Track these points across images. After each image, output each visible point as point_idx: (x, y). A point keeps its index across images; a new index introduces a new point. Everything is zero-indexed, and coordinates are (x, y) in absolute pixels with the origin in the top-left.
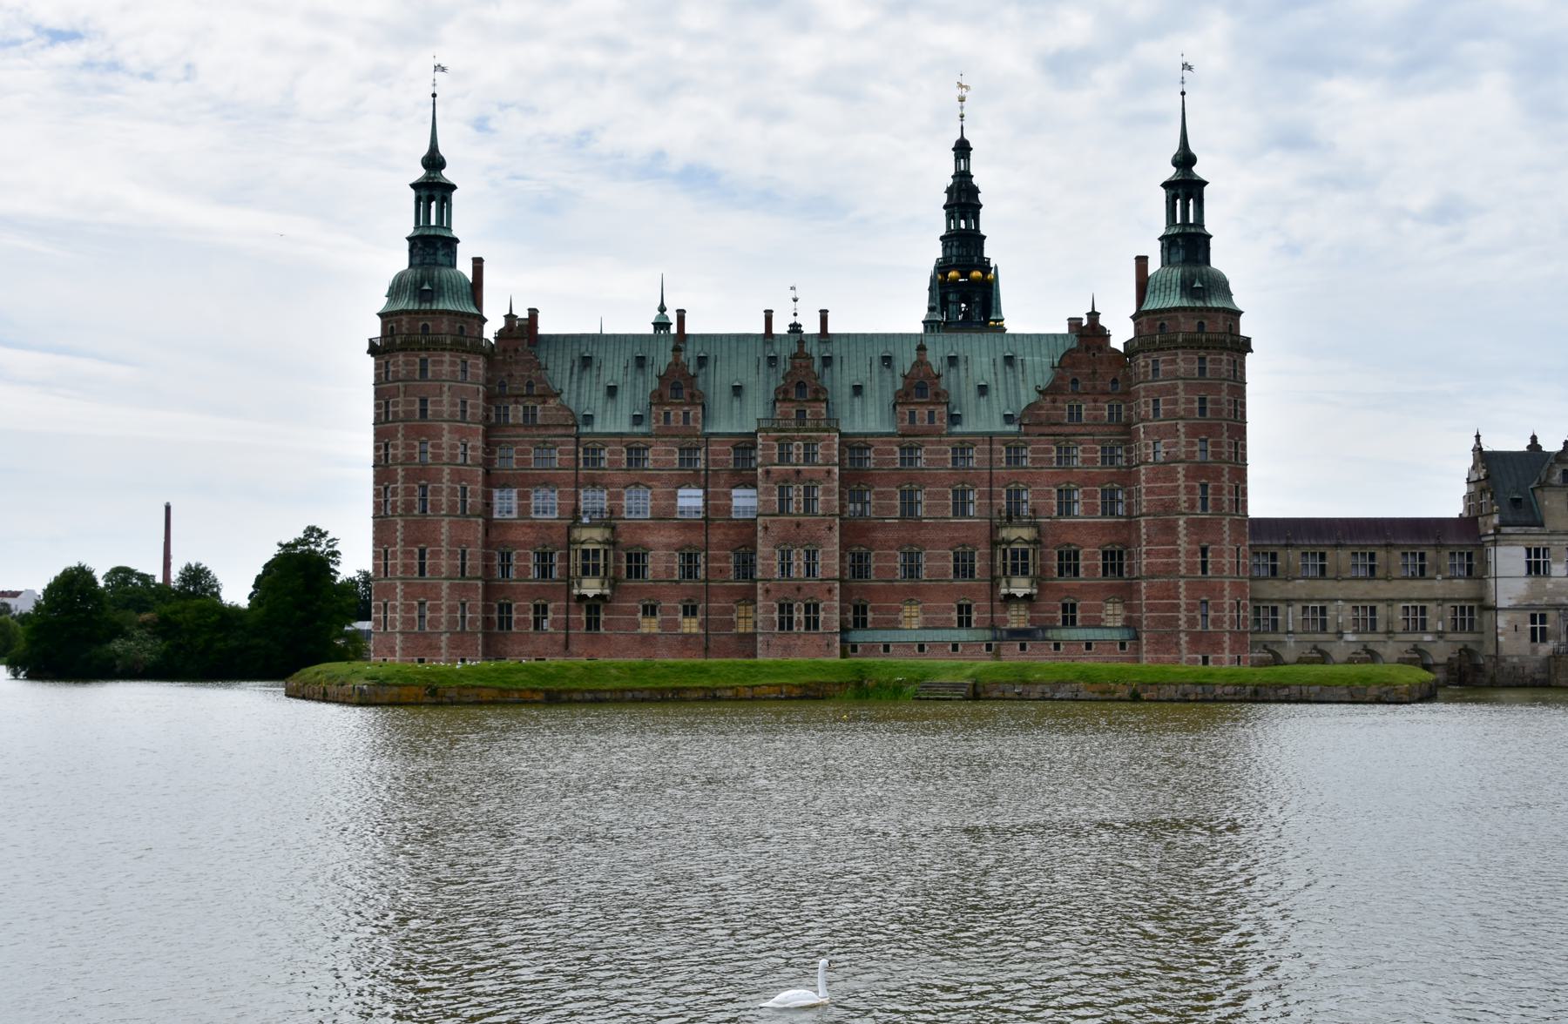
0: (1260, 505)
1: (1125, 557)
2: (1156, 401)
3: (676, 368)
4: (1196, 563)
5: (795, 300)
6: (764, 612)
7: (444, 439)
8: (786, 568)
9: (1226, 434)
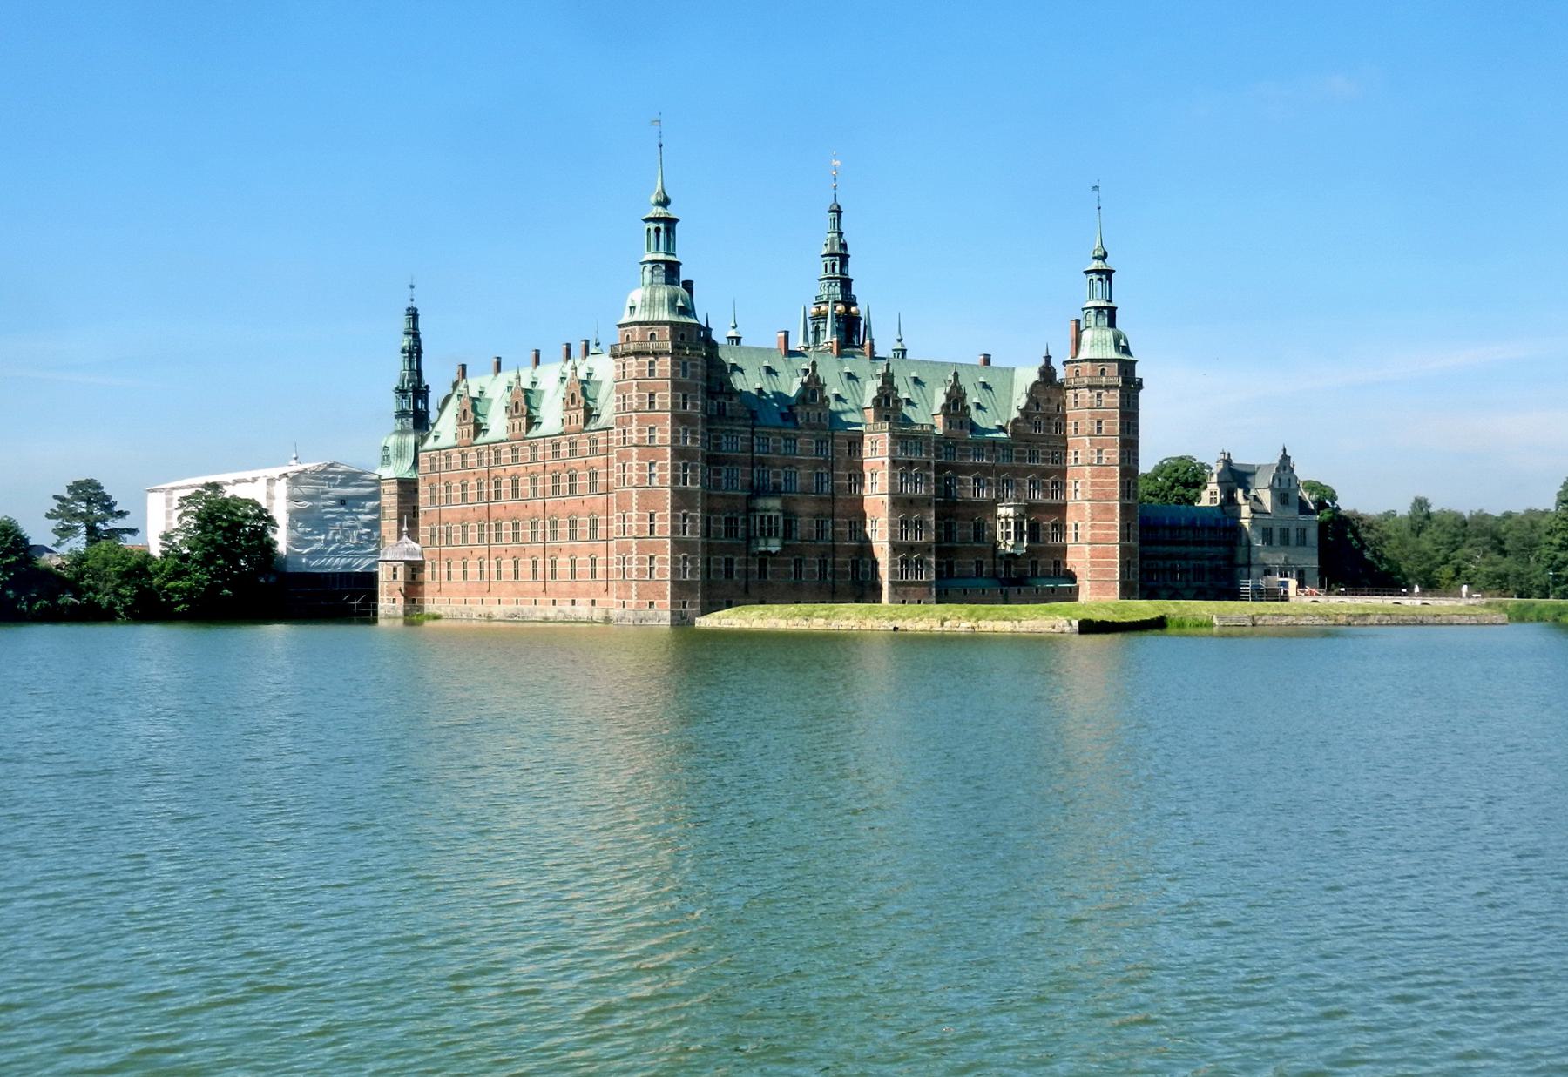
2: (1099, 422)
5: (412, 287)
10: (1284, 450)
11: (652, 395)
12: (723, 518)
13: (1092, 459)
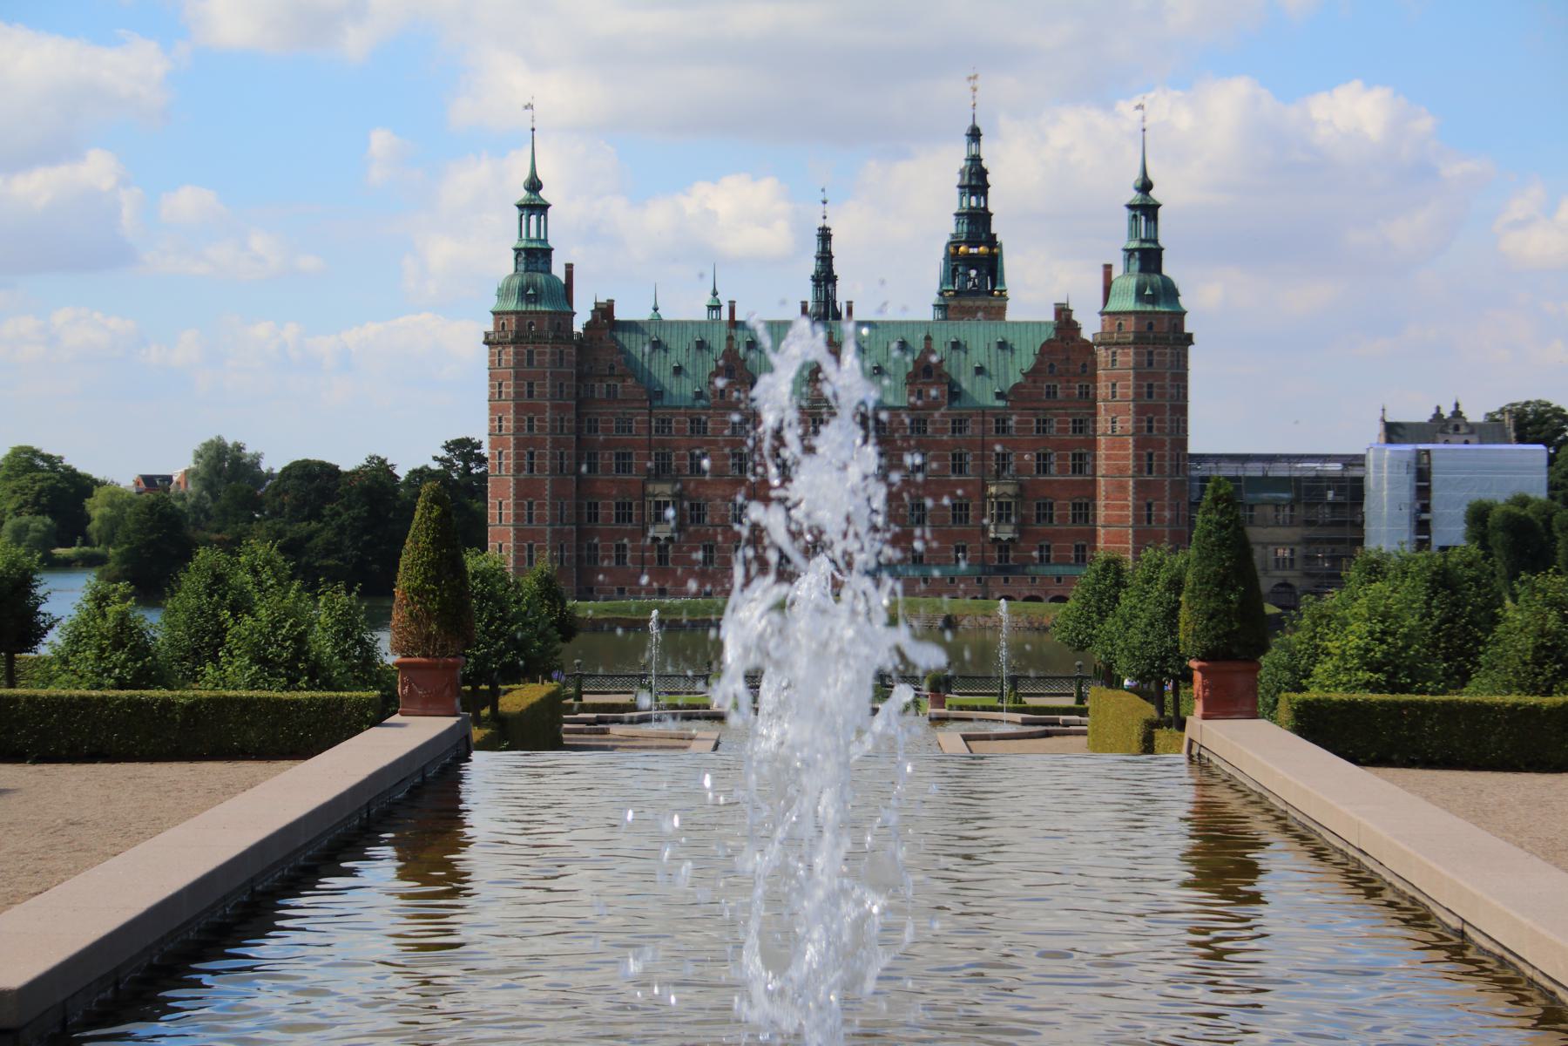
1: (1090, 508)
2: (1114, 385)
4: (1142, 515)
5: (825, 202)
7: (548, 414)
9: (1168, 414)
10: (1457, 405)
11: (500, 385)
12: (614, 503)
13: (1107, 427)
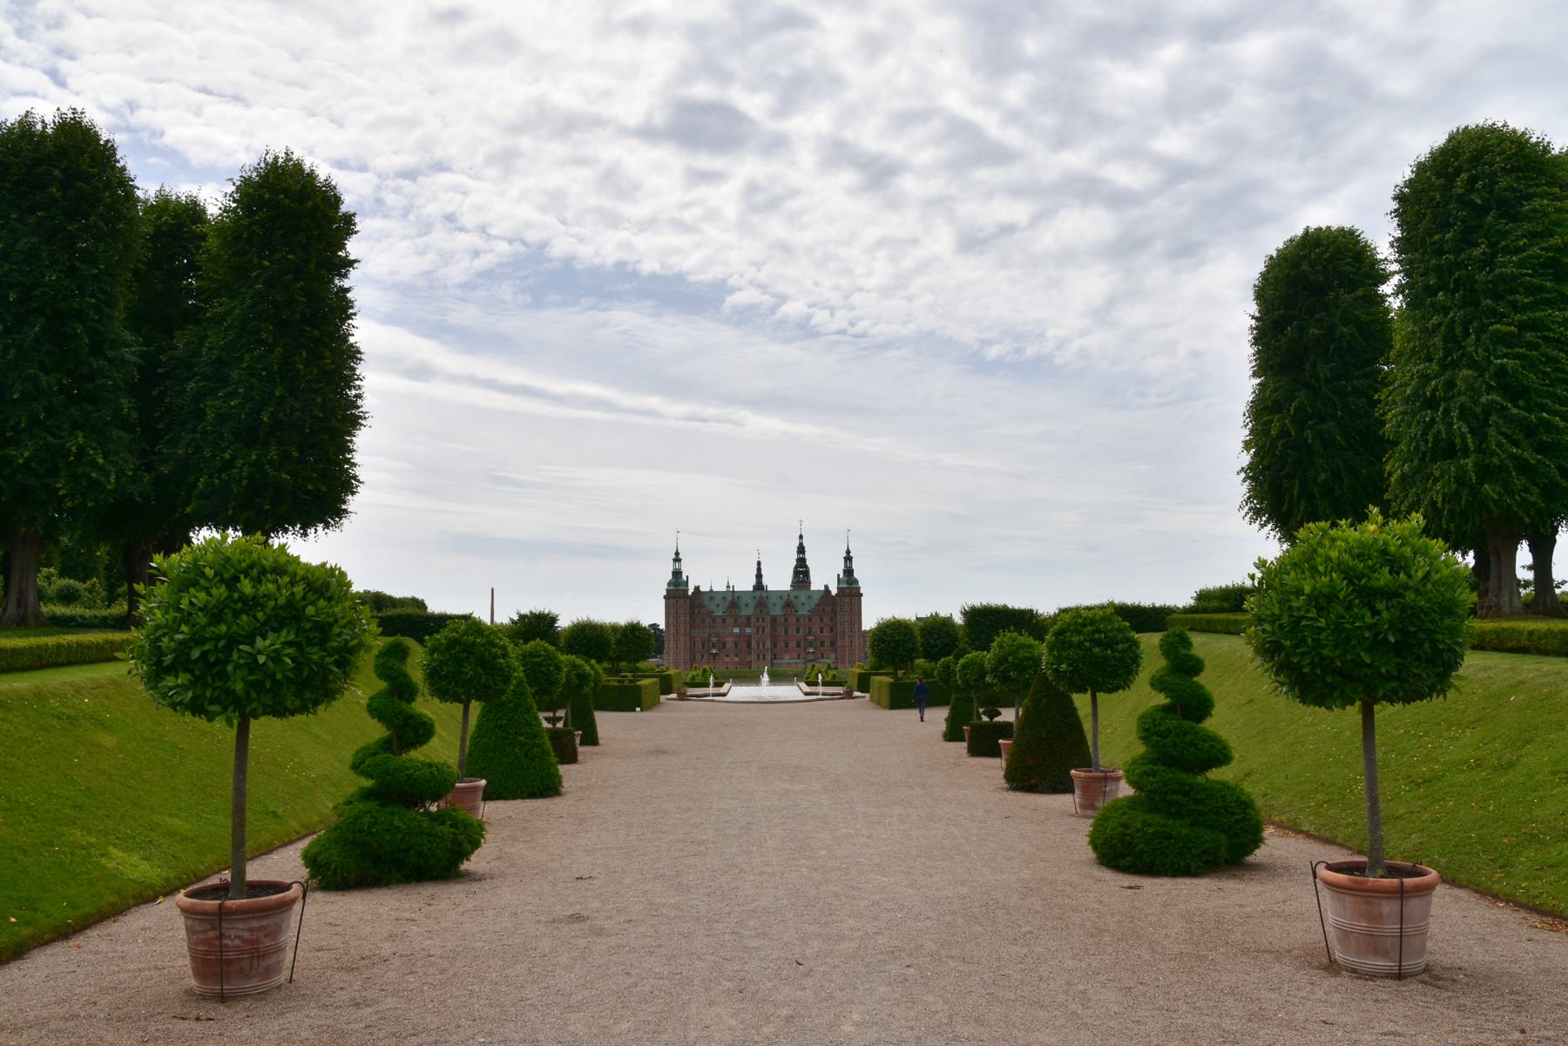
0: (863, 629)
3: (733, 599)
6: (754, 656)
8: (758, 646)
